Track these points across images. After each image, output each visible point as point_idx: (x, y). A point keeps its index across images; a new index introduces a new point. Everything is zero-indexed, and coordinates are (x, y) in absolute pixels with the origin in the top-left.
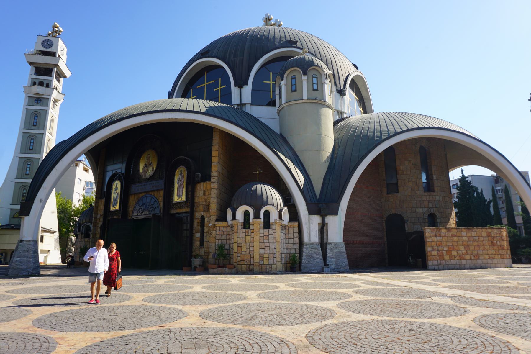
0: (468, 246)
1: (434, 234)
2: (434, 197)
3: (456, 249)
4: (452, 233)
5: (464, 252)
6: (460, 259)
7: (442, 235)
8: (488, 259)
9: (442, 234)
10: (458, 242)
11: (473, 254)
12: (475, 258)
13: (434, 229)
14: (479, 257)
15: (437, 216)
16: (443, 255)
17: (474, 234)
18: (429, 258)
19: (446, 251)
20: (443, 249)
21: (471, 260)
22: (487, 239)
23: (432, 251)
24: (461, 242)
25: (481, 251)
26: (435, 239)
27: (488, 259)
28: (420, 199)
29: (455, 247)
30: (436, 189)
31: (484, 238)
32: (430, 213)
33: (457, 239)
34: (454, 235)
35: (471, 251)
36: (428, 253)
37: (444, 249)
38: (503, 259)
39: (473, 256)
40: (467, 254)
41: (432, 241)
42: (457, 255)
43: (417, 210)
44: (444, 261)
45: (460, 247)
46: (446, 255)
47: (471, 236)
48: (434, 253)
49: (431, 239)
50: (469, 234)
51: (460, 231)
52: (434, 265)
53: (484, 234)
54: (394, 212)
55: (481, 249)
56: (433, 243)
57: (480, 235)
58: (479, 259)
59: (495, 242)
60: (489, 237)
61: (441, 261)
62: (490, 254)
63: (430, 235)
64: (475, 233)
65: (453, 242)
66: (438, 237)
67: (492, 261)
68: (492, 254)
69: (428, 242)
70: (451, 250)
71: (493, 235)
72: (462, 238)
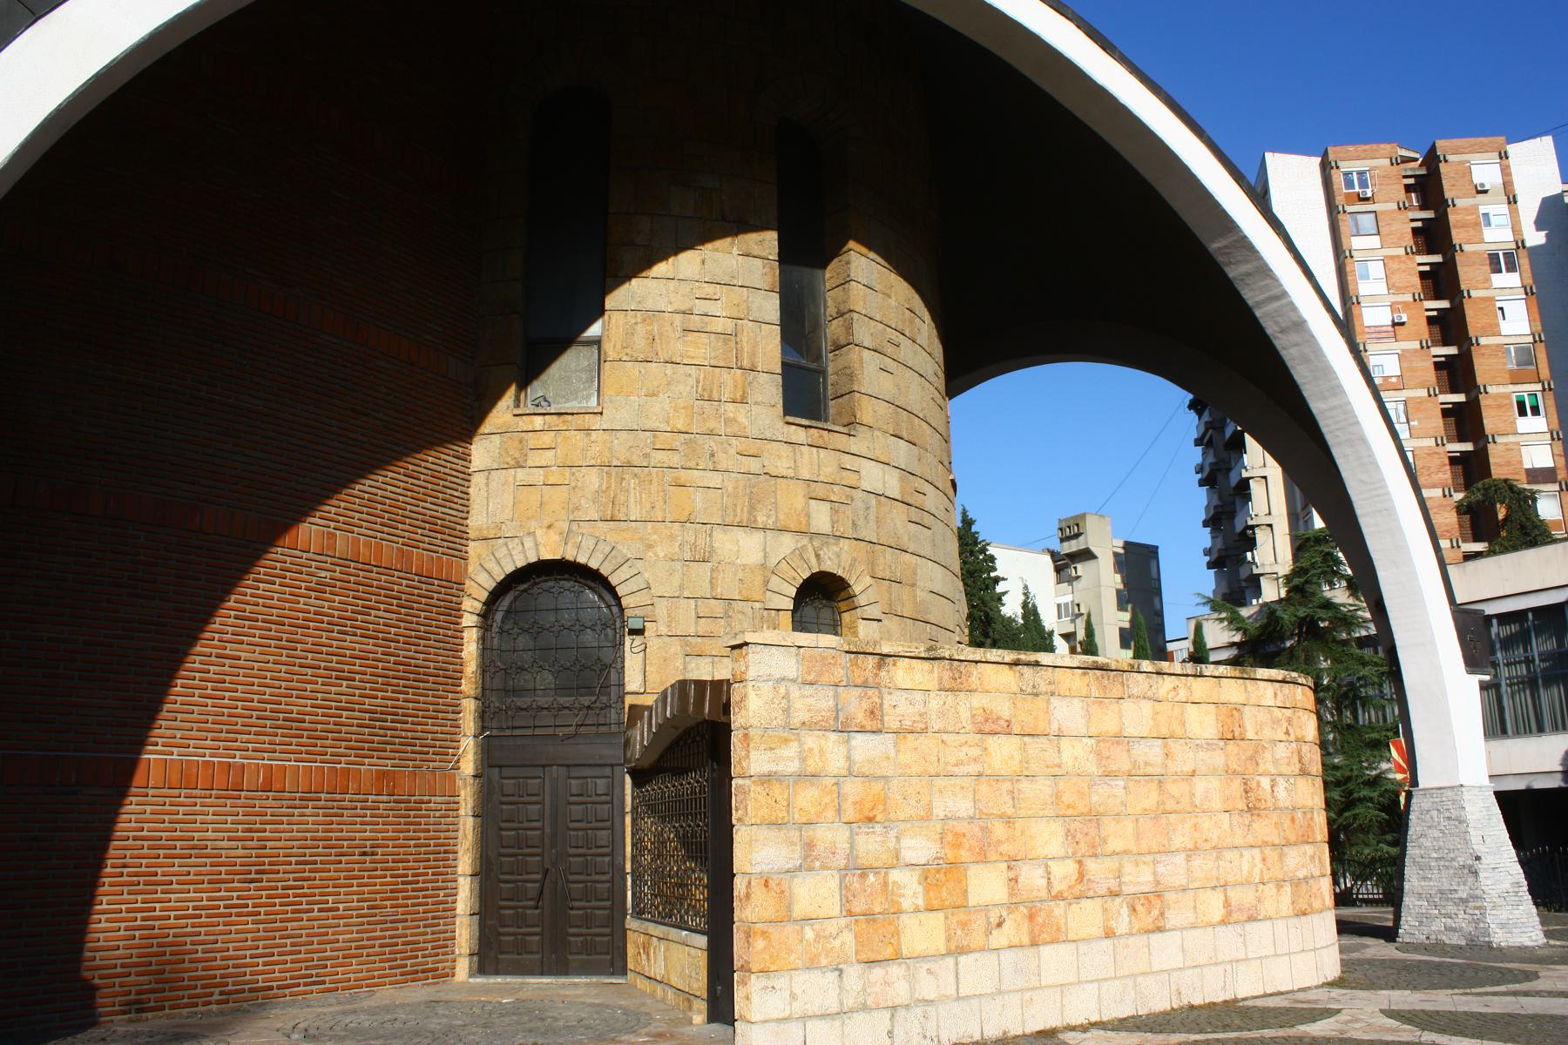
0: (1094, 816)
1: (831, 703)
2: (848, 461)
3: (1004, 848)
4: (977, 701)
6: (1034, 944)
7: (891, 722)
8: (1224, 922)
9: (899, 709)
10: (1025, 785)
11: (1133, 889)
14: (1162, 914)
15: (861, 600)
17: (1136, 716)
18: (760, 944)
21: (1107, 943)
22: (1218, 759)
24: (1041, 789)
25: (1180, 859)
26: (831, 753)
27: (1224, 922)
28: (754, 465)
29: (999, 830)
30: (868, 411)
31: (1201, 755)
32: (813, 575)
33: (1018, 757)
34: (999, 718)
36: (758, 893)
37: (909, 856)
38: (1304, 914)
39: (1125, 911)
40: (1081, 890)
42: (1012, 906)
44: (895, 970)
46: (917, 910)
47: (1119, 738)
49: (791, 750)
50: (1108, 721)
51: (1043, 688)
52: (805, 1018)
53: (1203, 723)
54: (550, 550)
56: (807, 798)
57: (1178, 731)
58: (1160, 929)
59: (1265, 783)
60: (1231, 745)
61: (877, 973)
62: (1231, 879)
63: (787, 711)
64: (1147, 707)
65: (984, 789)
67: (1244, 943)
68: (1247, 882)
69: (767, 779)
70: (964, 855)
71: (1250, 734)
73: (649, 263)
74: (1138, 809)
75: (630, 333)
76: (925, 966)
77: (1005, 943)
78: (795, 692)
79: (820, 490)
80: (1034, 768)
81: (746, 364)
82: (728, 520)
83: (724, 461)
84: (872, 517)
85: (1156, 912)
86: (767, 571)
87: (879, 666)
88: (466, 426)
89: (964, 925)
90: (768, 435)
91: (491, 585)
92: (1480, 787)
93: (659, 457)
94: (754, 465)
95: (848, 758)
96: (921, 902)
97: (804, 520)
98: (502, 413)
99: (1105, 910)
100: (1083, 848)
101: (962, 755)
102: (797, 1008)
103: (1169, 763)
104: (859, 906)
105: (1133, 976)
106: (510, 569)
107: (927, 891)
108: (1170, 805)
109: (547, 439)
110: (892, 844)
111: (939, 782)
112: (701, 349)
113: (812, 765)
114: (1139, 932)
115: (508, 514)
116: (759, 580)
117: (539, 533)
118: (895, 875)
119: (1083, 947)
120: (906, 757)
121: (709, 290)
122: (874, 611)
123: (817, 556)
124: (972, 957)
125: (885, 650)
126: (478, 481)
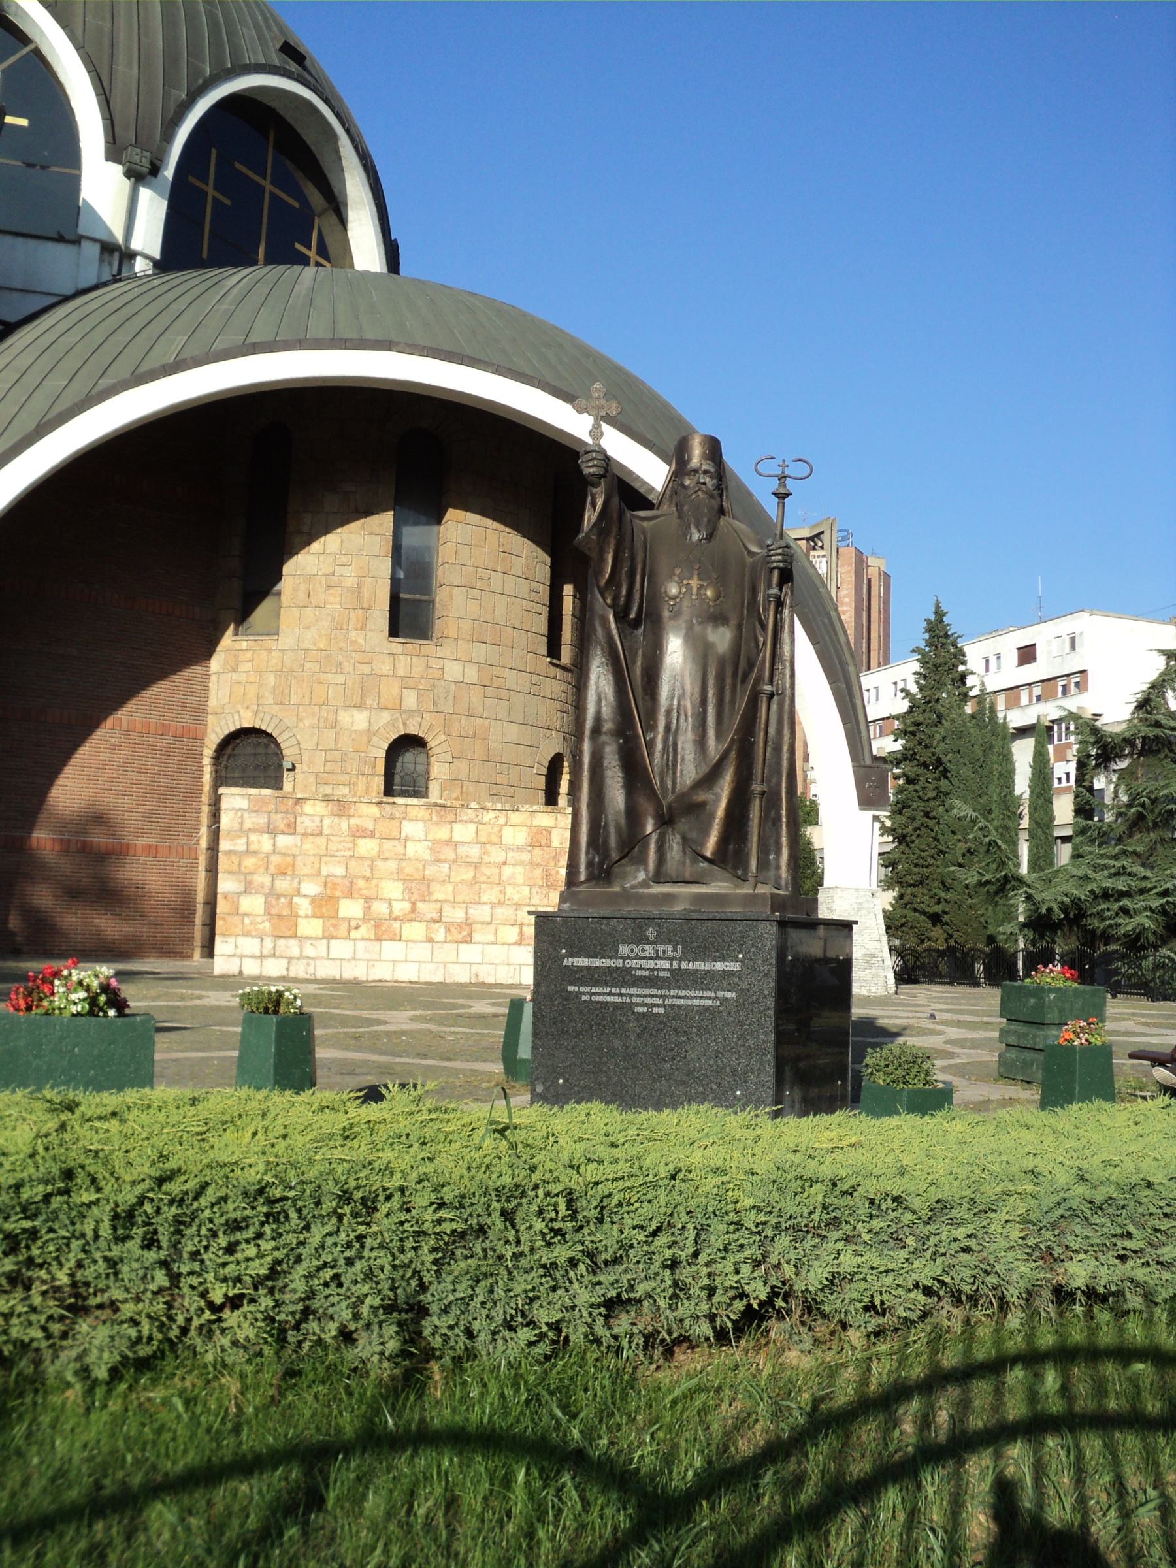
0: (426, 882)
2: (433, 663)
3: (364, 892)
4: (353, 821)
5: (401, 907)
6: (378, 939)
7: (299, 829)
8: (515, 944)
9: (305, 823)
10: (379, 863)
11: (448, 920)
12: (449, 938)
13: (263, 801)
14: (470, 934)
16: (294, 916)
17: (463, 832)
19: (314, 900)
20: (298, 891)
21: (429, 945)
22: (526, 857)
23: (239, 894)
24: (392, 865)
25: (487, 908)
26: (264, 843)
27: (515, 944)
28: (366, 669)
29: (361, 883)
31: (511, 854)
35: (438, 905)
39: (442, 930)
40: (413, 915)
41: (248, 852)
42: (365, 920)
43: (345, 717)
44: (293, 943)
45: (383, 884)
47: (449, 842)
48: (253, 904)
50: (442, 833)
51: (397, 815)
52: (241, 957)
53: (516, 836)
55: (485, 898)
56: (249, 862)
57: (495, 839)
60: (537, 851)
61: (282, 942)
63: (242, 823)
64: (472, 827)
65: (353, 863)
66: (283, 833)
70: (338, 894)
72: (400, 849)
73: (309, 543)
74: (458, 880)
75: (296, 589)
76: (310, 942)
77: (359, 936)
78: (246, 815)
79: (411, 683)
80: (387, 855)
81: (365, 605)
82: (347, 703)
83: (347, 667)
84: (451, 697)
85: (465, 933)
86: (370, 733)
87: (296, 804)
88: (206, 650)
89: (334, 926)
90: (377, 650)
91: (217, 741)
92: (857, 889)
93: (308, 665)
94: (366, 669)
95: (274, 845)
96: (309, 913)
97: (398, 702)
98: (228, 640)
99: (427, 928)
100: (416, 896)
101: (341, 846)
102: (238, 952)
103: (485, 857)
104: (274, 911)
105: (445, 963)
106: (227, 732)
107: (313, 908)
108: (483, 879)
109: (249, 655)
110: (295, 884)
111: (324, 859)
112: (334, 599)
113: (253, 847)
114: (450, 942)
115: (227, 700)
116: (365, 739)
117: (242, 711)
118: (295, 900)
119: (410, 944)
120: (307, 846)
121: (344, 559)
122: (442, 757)
123: (405, 724)
124: (338, 941)
125: (299, 796)
126: (213, 679)
